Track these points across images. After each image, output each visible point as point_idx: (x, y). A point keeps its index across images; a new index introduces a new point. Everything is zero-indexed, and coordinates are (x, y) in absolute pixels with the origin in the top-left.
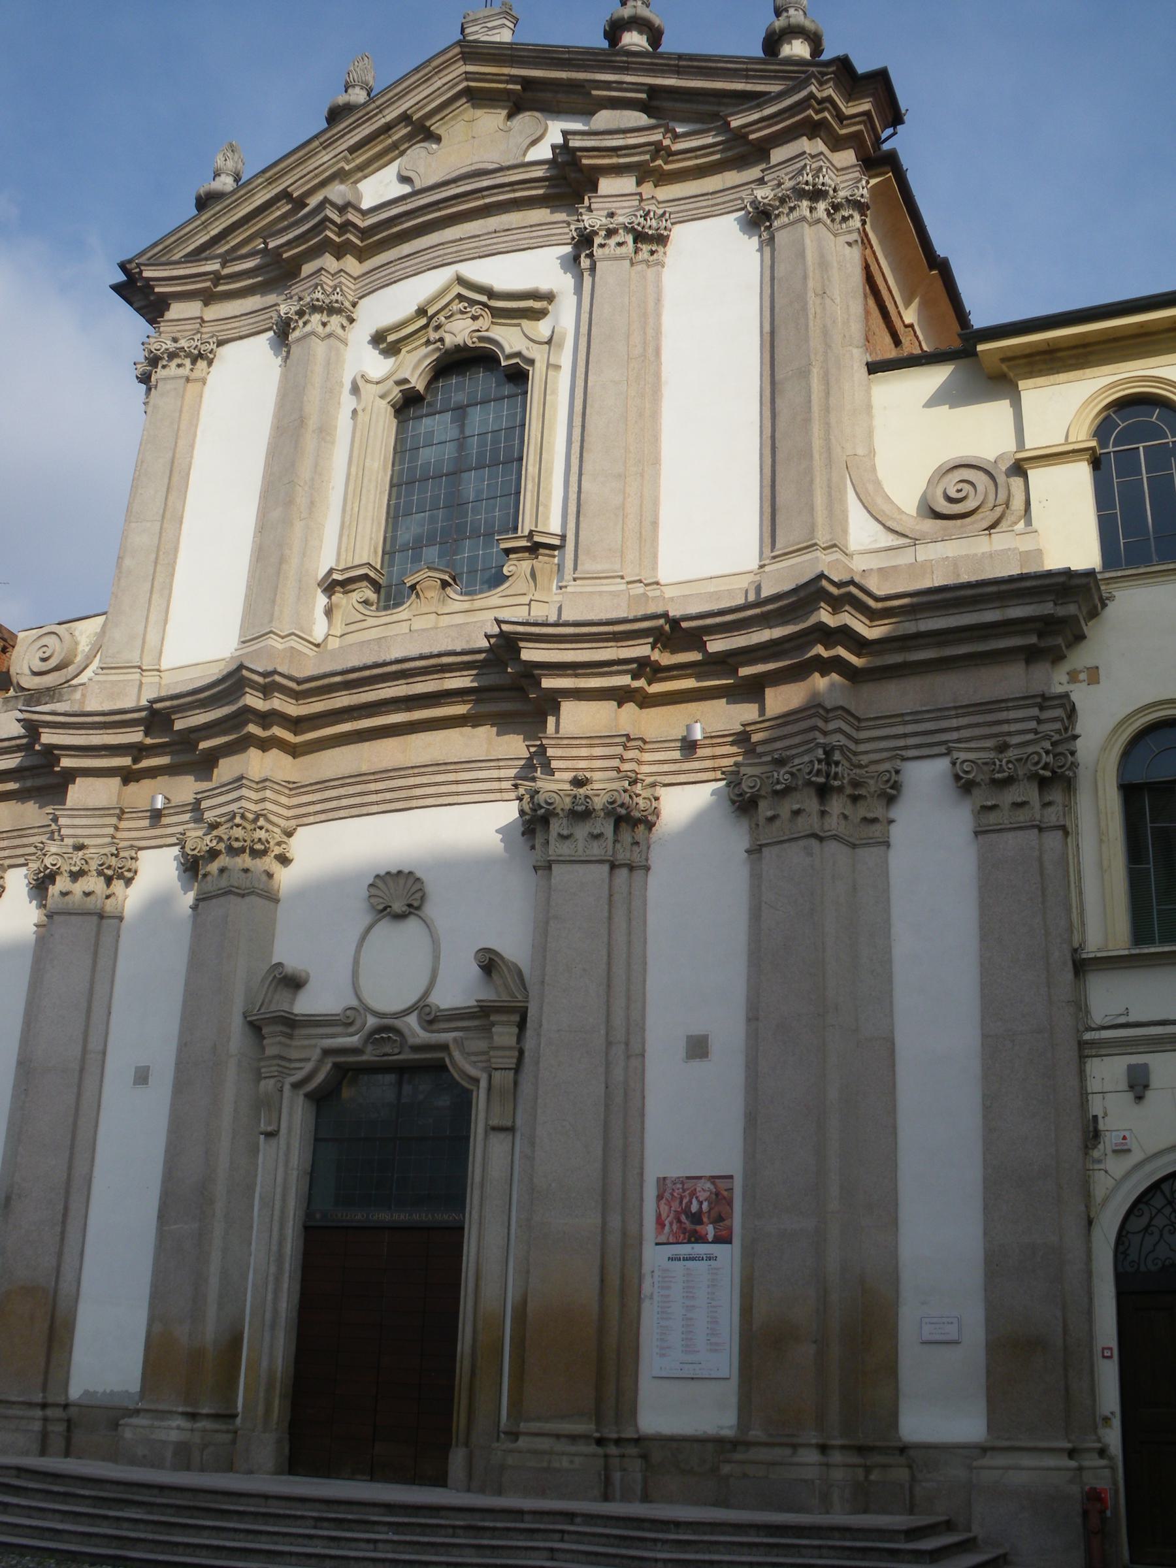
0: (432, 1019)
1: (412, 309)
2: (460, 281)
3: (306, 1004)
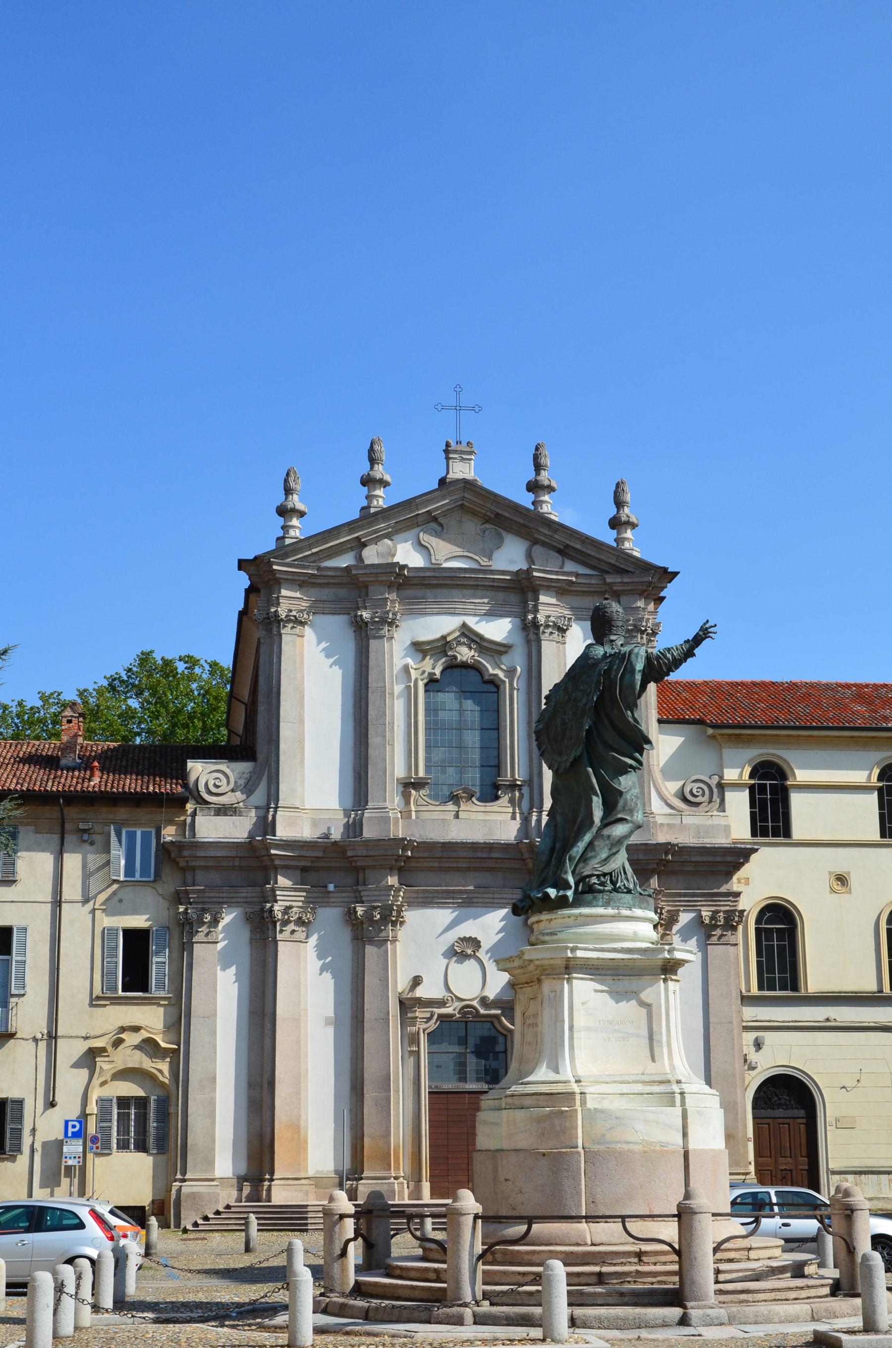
0: (484, 1001)
1: (438, 635)
2: (464, 625)
3: (421, 992)
